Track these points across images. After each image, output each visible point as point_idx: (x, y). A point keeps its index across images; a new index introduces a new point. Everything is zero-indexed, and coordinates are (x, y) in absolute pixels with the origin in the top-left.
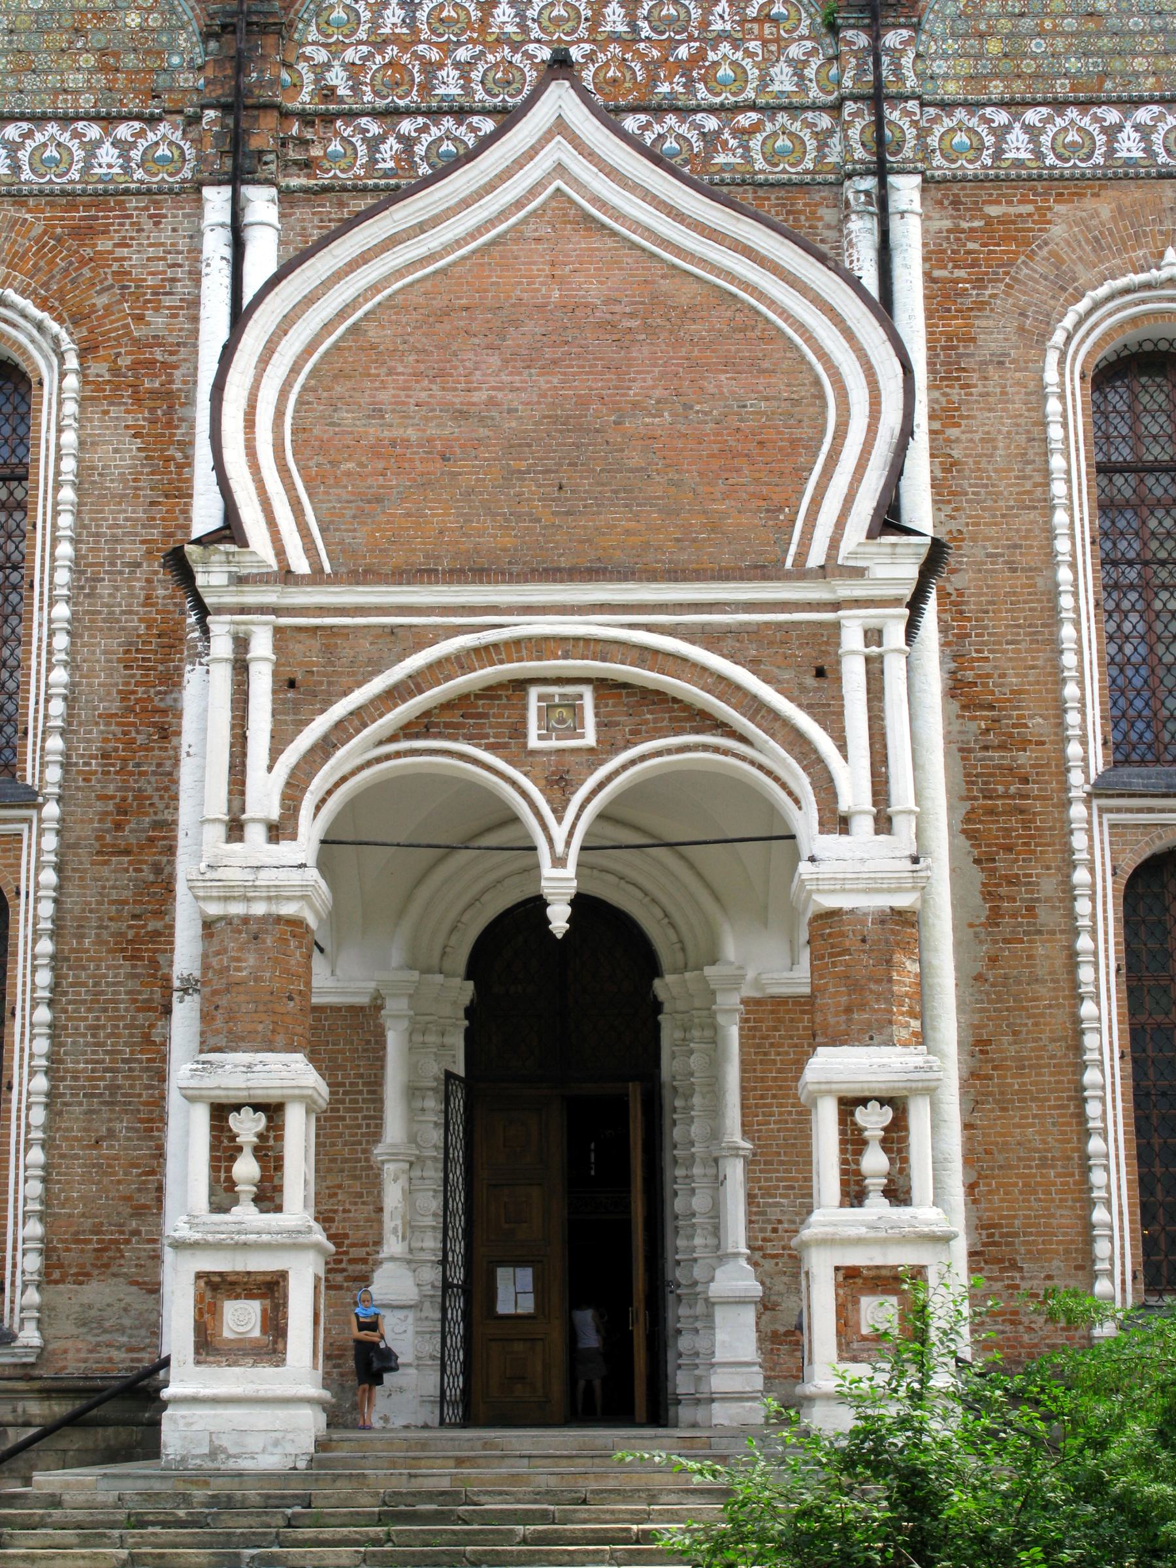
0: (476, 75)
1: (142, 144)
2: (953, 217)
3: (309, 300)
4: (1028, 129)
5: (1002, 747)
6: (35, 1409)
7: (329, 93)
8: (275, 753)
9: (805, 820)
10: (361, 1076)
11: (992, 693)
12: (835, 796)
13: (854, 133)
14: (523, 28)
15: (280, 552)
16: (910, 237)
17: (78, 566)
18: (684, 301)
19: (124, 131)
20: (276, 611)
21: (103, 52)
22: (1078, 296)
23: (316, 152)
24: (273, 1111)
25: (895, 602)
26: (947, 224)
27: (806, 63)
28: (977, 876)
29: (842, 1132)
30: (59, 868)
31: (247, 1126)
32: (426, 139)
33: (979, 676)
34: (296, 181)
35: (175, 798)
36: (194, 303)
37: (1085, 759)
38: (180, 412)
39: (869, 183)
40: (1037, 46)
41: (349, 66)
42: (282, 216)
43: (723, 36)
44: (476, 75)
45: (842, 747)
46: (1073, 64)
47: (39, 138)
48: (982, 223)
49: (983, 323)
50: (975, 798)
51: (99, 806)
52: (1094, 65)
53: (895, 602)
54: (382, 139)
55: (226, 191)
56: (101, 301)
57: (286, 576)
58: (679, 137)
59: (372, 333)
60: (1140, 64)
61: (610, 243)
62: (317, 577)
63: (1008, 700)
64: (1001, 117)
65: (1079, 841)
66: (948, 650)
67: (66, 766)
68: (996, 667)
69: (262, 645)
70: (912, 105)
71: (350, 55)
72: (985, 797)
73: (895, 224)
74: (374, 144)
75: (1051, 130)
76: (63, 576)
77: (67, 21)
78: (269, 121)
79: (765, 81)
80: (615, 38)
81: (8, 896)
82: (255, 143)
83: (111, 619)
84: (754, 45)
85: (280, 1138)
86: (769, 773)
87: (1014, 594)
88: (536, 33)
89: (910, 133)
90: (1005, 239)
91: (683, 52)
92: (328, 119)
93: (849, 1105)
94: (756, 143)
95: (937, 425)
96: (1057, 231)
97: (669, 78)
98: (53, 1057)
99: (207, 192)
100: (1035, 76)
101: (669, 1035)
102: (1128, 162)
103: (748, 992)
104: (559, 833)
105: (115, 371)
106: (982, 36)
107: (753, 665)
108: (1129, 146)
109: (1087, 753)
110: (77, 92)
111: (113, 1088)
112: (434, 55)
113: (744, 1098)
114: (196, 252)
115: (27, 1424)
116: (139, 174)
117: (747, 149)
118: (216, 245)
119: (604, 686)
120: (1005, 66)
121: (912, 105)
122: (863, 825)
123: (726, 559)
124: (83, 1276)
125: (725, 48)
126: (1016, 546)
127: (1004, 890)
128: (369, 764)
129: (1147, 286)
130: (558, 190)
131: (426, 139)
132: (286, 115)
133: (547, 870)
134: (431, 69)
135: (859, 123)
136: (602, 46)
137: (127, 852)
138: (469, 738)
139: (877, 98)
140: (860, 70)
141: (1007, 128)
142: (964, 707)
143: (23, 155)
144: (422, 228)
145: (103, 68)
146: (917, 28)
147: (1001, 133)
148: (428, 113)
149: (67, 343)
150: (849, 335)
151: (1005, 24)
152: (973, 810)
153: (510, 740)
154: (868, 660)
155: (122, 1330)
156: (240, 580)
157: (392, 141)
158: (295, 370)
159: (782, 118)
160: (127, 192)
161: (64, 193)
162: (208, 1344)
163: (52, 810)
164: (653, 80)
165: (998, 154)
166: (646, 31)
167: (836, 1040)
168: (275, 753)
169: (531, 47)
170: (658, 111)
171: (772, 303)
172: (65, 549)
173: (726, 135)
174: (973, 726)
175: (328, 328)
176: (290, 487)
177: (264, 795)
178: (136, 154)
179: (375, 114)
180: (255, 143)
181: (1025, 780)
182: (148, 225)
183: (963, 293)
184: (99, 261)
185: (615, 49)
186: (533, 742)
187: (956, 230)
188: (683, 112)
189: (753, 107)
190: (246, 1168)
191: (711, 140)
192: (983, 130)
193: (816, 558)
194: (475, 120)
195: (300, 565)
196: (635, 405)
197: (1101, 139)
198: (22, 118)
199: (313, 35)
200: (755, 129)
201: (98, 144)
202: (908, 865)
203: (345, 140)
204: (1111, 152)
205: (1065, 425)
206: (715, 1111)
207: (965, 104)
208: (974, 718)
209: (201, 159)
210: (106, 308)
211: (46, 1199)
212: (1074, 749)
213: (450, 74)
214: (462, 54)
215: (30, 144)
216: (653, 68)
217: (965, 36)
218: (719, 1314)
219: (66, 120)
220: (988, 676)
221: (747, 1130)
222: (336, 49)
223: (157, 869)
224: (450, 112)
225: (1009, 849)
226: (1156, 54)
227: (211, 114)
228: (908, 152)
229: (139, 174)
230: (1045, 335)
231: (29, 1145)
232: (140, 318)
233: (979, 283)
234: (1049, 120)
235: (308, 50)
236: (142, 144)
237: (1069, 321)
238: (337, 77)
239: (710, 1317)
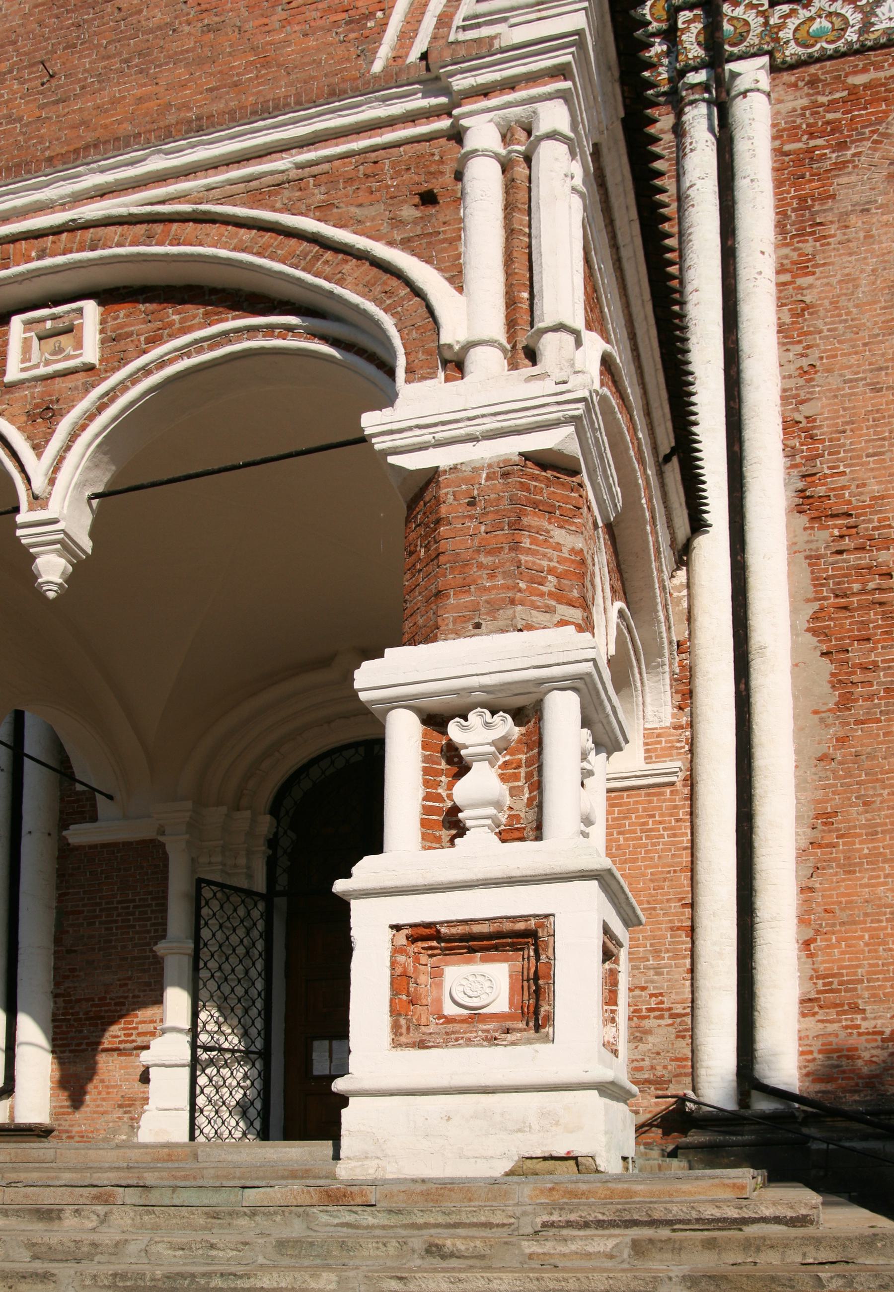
2: (808, 95)
10: (150, 893)
11: (849, 502)
26: (805, 102)
33: (833, 489)
48: (845, 93)
49: (844, 180)
50: (825, 598)
63: (870, 506)
66: (795, 472)
68: (853, 479)
72: (837, 596)
87: (878, 411)
95: (787, 277)
126: (881, 369)
152: (822, 609)
174: (824, 535)
187: (815, 105)
208: (828, 527)
220: (843, 488)
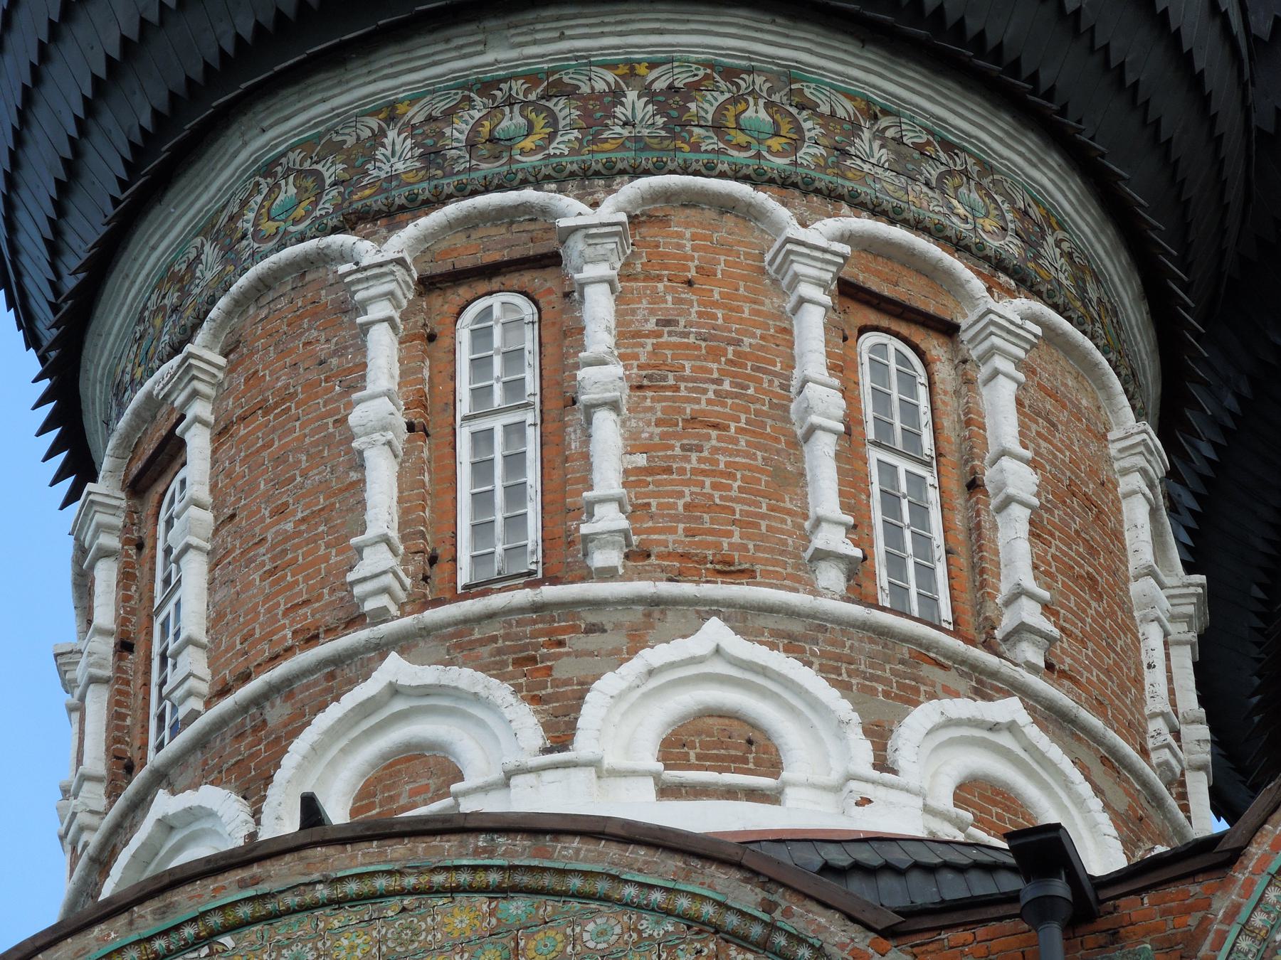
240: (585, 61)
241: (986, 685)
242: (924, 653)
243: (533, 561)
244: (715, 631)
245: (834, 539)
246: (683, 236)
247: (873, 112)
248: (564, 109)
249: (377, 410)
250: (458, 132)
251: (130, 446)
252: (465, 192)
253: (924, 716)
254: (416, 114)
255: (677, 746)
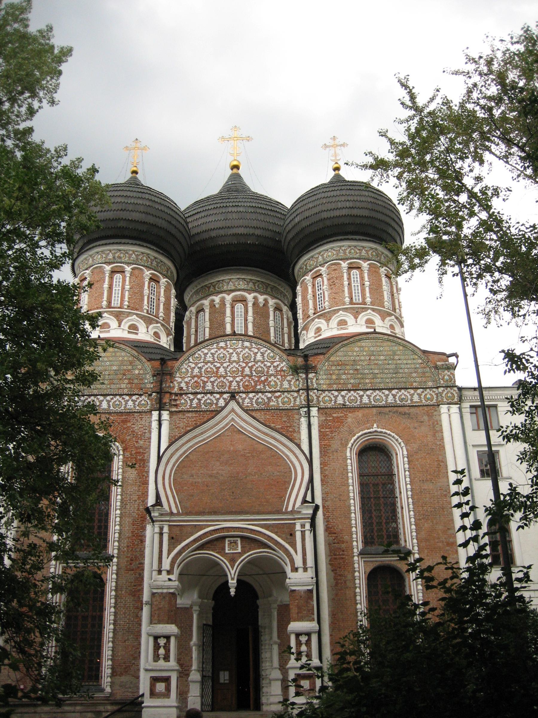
0: (215, 384)
1: (138, 401)
3: (177, 450)
4: (342, 396)
5: (338, 543)
6: (109, 708)
7: (181, 389)
8: (169, 554)
9: (288, 569)
12: (294, 563)
13: (302, 398)
14: (226, 374)
15: (170, 508)
16: (315, 422)
17: (122, 501)
18: (260, 450)
19: (134, 398)
20: (169, 521)
21: (129, 379)
22: (354, 435)
23: (178, 402)
24: (168, 638)
25: (308, 518)
26: (324, 418)
27: (291, 381)
28: (332, 574)
29: (296, 642)
30: (117, 574)
31: (162, 642)
32: (204, 399)
34: (174, 409)
35: (144, 557)
36: (150, 438)
37: (357, 546)
38: (146, 464)
39: (306, 409)
40: (344, 377)
41: (186, 382)
42: (170, 417)
43: (272, 375)
44: (215, 384)
45: (296, 552)
46: (352, 381)
47: (115, 399)
51: (126, 559)
52: (357, 381)
53: (308, 518)
54: (194, 399)
55: (157, 412)
56: (128, 438)
57: (172, 514)
58: (262, 399)
59: (191, 457)
60: (367, 381)
61: (244, 436)
62: (178, 514)
64: (336, 393)
65: (356, 565)
67: (119, 549)
69: (166, 529)
70: (315, 391)
71: (186, 380)
73: (312, 418)
74: (191, 401)
75: (347, 396)
76: (118, 504)
77: (122, 372)
78: (168, 395)
79: (282, 385)
80: (247, 375)
81: (105, 581)
82: (164, 401)
83: (130, 514)
84: (279, 377)
85: (169, 644)
86: (280, 558)
88: (229, 374)
89: (315, 397)
90: (338, 422)
91: (263, 379)
92: (181, 395)
93: (298, 635)
94: (280, 400)
96: (349, 420)
97: (260, 385)
98: (115, 620)
99: (153, 412)
100: (343, 384)
101: (260, 614)
102: (365, 404)
103: (278, 603)
104: (233, 572)
105: (131, 454)
106: (331, 374)
107: (276, 533)
108: (365, 400)
109: (358, 544)
110: (124, 389)
111: (129, 628)
112: (206, 380)
113: (278, 630)
114: (150, 426)
115: (108, 712)
116: (137, 408)
117: (278, 401)
118: (155, 425)
119: (242, 538)
120: (337, 381)
121: (315, 391)
122: (301, 570)
123: (270, 509)
124: (121, 675)
125: (273, 377)
127: (339, 578)
128: (190, 556)
129: (370, 433)
130: (233, 418)
131: (204, 399)
132: (171, 394)
133: (230, 581)
134: (205, 383)
135: (303, 395)
136: (244, 377)
137: (133, 570)
138: (212, 550)
139: (307, 389)
140: (303, 383)
141: (337, 396)
142: (329, 534)
143: (111, 403)
144: (202, 433)
145: (129, 383)
146: (316, 373)
147: (336, 397)
148: (204, 393)
149: (120, 448)
150: (297, 457)
151: (337, 372)
153: (222, 551)
154: (302, 531)
155: (130, 688)
156: (161, 515)
157: (196, 400)
158: (174, 466)
159: (286, 394)
160: (135, 412)
161: (120, 412)
162: (153, 694)
163: (115, 560)
164: (256, 385)
165: (335, 402)
166: (254, 374)
167: (295, 620)
168: (169, 554)
169: (228, 378)
170: (257, 392)
171: (280, 450)
172: (119, 497)
173: (273, 398)
174: (331, 538)
175: (181, 456)
176: (172, 493)
177: (166, 565)
178: (137, 403)
179: (192, 393)
180: (164, 401)
181: (343, 551)
182: (139, 420)
183: (328, 435)
184: (129, 428)
185: (247, 378)
186: (227, 551)
188: (263, 392)
189: (279, 391)
190: (162, 651)
191: (269, 399)
192: (332, 396)
193: (290, 509)
194: (215, 395)
195: (175, 511)
196: (250, 474)
197: (359, 398)
198: (111, 395)
199: (178, 375)
200: (280, 396)
201: (128, 401)
202: (310, 579)
203: (185, 400)
204: (361, 401)
205: (352, 466)
206: (271, 633)
207: (327, 390)
209: (152, 405)
210: (130, 439)
211: (113, 655)
212: (355, 543)
213: (209, 384)
214: (212, 379)
215: (113, 401)
216: (256, 382)
217: (327, 375)
218: (272, 682)
219: (121, 395)
221: (279, 637)
222: (183, 378)
223: (140, 574)
224: (209, 393)
225: (340, 568)
226: (371, 379)
227: (154, 394)
228: (314, 402)
229: (137, 408)
230: (347, 445)
231: (109, 642)
232: (137, 442)
233: (332, 432)
234: (347, 394)
235: (177, 379)
236: (138, 401)
237: (352, 441)
238: (183, 385)
239: (270, 683)
240: (130, 250)
241: (157, 322)
242: (153, 319)
243: (119, 305)
244: (135, 316)
245: (146, 307)
246: (136, 272)
247: (156, 258)
248: (127, 255)
249: (106, 285)
250: (117, 255)
251: (81, 277)
252: (117, 263)
253: (151, 326)
254: (113, 252)
255: (130, 327)
